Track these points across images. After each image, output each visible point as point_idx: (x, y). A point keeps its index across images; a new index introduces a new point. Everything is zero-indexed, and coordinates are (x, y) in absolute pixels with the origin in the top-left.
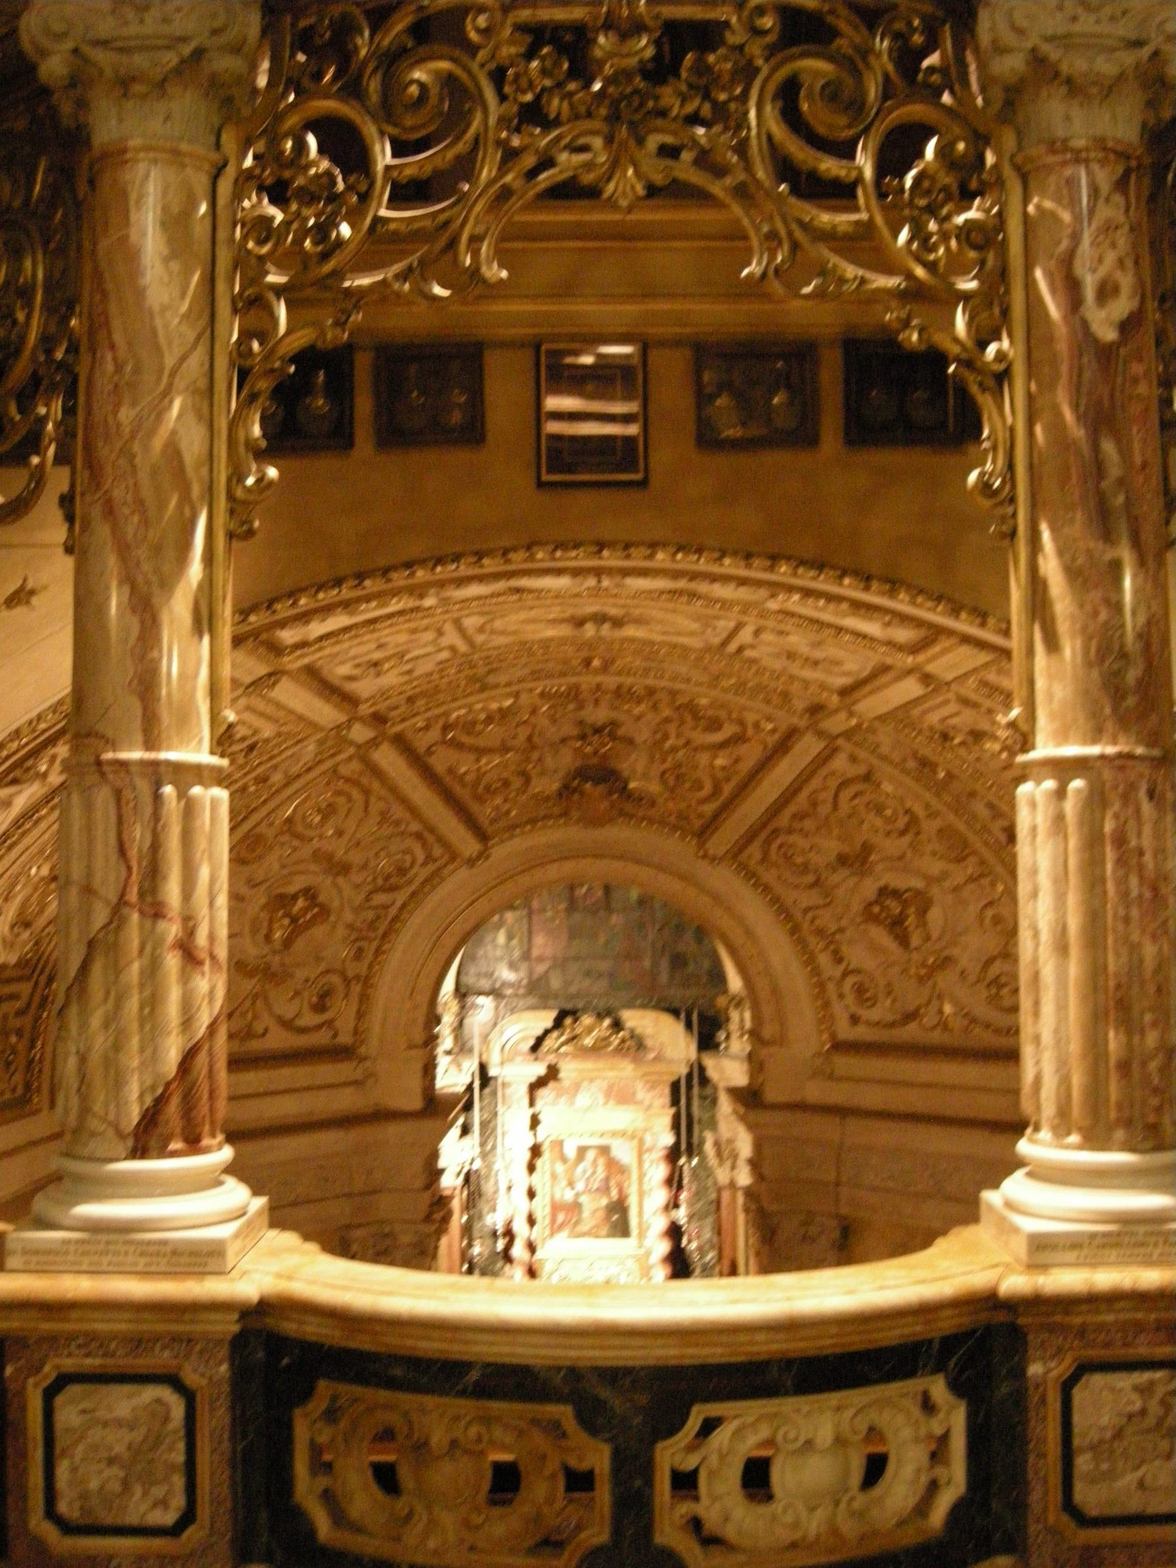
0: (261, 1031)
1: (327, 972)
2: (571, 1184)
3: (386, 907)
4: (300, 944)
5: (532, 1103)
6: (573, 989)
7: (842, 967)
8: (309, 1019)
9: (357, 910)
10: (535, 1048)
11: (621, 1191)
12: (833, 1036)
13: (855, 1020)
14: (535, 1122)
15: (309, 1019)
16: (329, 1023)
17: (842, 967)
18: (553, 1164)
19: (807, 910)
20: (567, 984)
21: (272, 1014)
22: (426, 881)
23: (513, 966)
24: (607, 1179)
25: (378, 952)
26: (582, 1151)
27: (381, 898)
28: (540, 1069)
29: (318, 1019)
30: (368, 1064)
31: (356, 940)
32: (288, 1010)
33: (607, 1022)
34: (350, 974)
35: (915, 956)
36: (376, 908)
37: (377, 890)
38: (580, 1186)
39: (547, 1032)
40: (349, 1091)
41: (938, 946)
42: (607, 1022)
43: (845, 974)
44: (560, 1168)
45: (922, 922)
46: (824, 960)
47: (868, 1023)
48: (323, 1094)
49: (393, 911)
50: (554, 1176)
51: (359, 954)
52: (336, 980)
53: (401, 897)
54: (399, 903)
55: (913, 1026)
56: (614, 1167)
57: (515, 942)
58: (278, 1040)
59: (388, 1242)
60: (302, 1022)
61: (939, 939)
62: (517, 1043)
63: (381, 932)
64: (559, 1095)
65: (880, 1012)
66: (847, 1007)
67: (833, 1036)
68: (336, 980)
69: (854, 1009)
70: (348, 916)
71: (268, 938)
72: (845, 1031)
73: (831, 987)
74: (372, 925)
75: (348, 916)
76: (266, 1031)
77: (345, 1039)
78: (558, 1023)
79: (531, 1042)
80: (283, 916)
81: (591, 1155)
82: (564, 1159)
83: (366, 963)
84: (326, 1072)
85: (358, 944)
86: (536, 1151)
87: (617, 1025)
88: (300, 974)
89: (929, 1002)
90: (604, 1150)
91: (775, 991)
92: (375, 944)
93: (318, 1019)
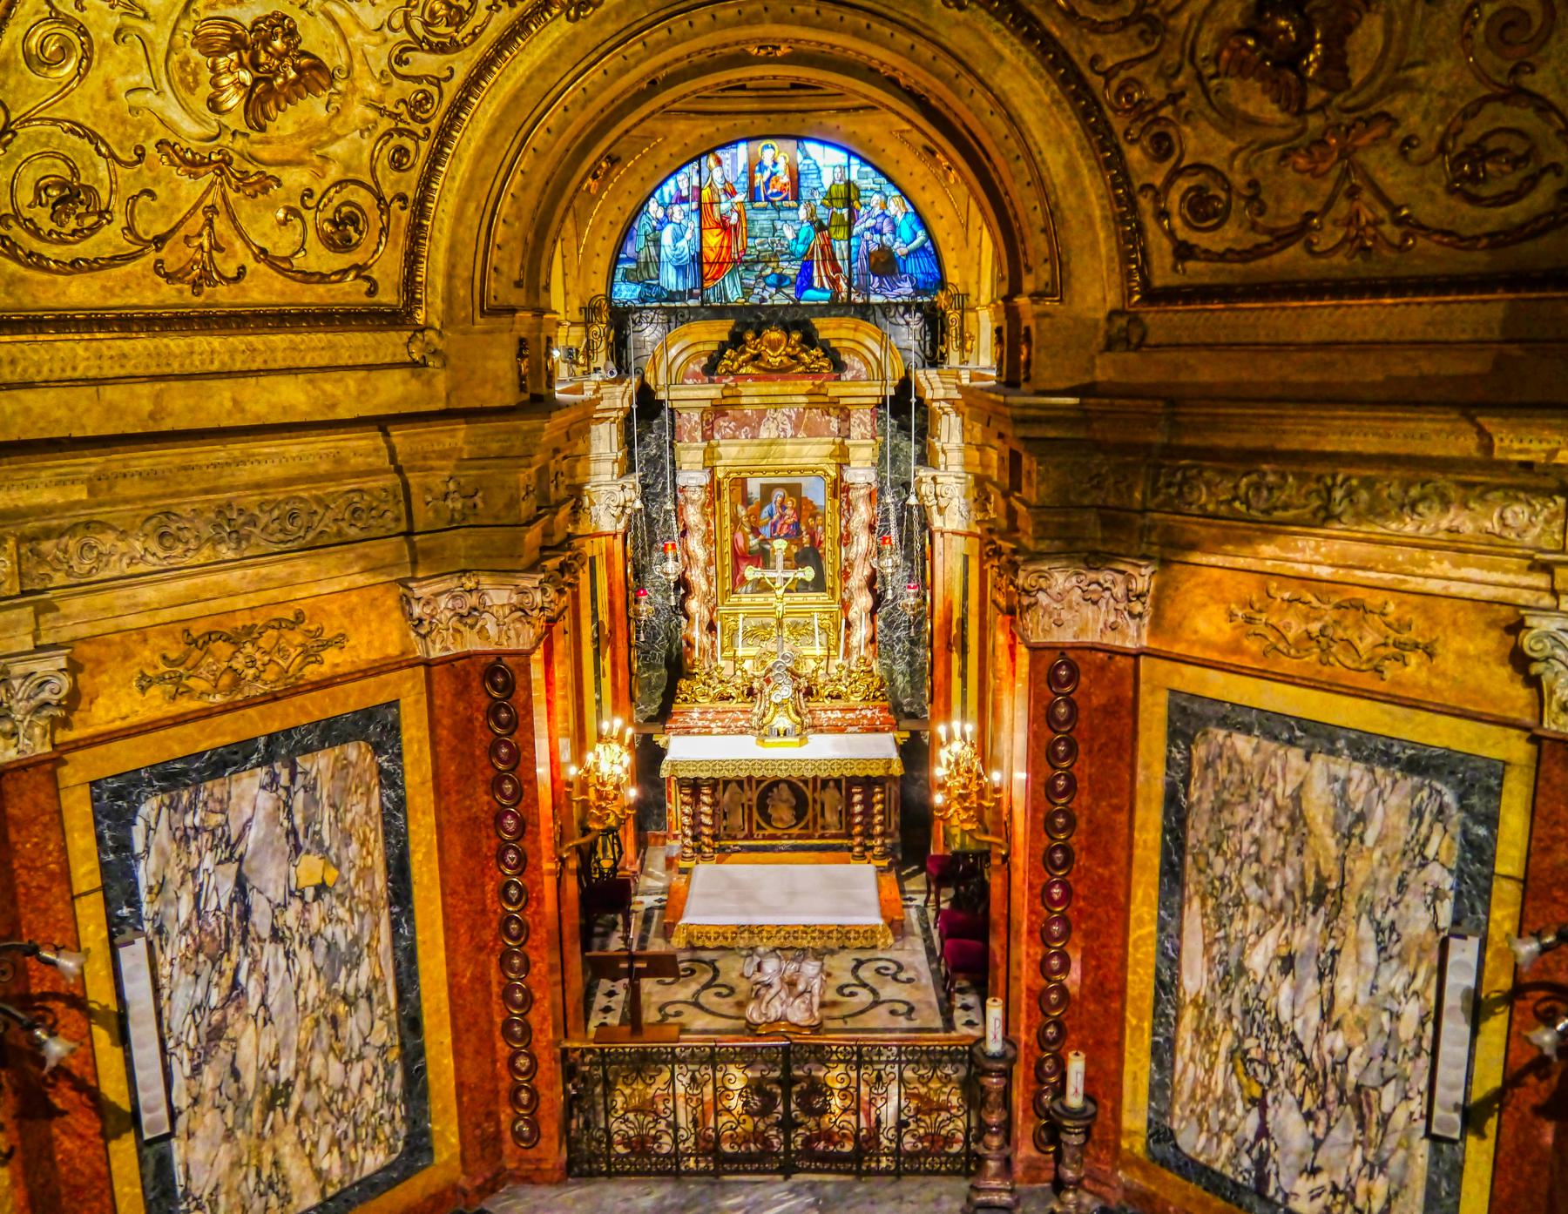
0: (232, 274)
1: (341, 184)
2: (755, 531)
3: (437, 82)
4: (285, 122)
5: (705, 438)
6: (754, 300)
7: (1168, 165)
8: (319, 258)
9: (384, 79)
10: (710, 369)
11: (812, 537)
12: (1146, 283)
13: (1184, 252)
14: (710, 457)
15: (319, 258)
16: (360, 269)
17: (1168, 165)
18: (733, 504)
19: (1108, 75)
20: (747, 291)
21: (248, 243)
22: (505, 42)
23: (680, 269)
24: (797, 524)
25: (436, 158)
26: (767, 490)
27: (424, 62)
28: (714, 392)
29: (341, 261)
30: (430, 334)
31: (389, 134)
32: (282, 243)
33: (796, 336)
34: (388, 193)
35: (1315, 122)
36: (417, 79)
37: (419, 44)
38: (766, 532)
39: (723, 346)
40: (398, 375)
41: (1362, 97)
42: (796, 336)
43: (1169, 181)
44: (742, 512)
45: (1336, 63)
46: (1134, 154)
47: (1209, 256)
48: (352, 380)
49: (451, 89)
50: (735, 520)
51: (399, 160)
52: (363, 198)
53: (462, 65)
54: (458, 79)
55: (1294, 251)
56: (804, 508)
57: (683, 244)
58: (264, 288)
59: (473, 600)
60: (299, 262)
61: (1371, 78)
62: (688, 361)
63: (433, 125)
64: (739, 428)
65: (1230, 235)
66: (1171, 233)
67: (1146, 283)
68: (363, 198)
69: (1183, 234)
70: (373, 89)
71: (214, 105)
72: (1163, 272)
73: (1145, 203)
74: (417, 107)
75: (373, 89)
76: (242, 271)
77: (388, 297)
78: (736, 341)
79: (705, 360)
80: (241, 65)
81: (778, 495)
82: (746, 501)
83: (415, 174)
84: (354, 344)
85: (396, 140)
86: (714, 489)
87: (809, 339)
88: (295, 178)
89: (1328, 205)
90: (794, 490)
91: (1053, 213)
92: (425, 146)
93: (341, 261)
